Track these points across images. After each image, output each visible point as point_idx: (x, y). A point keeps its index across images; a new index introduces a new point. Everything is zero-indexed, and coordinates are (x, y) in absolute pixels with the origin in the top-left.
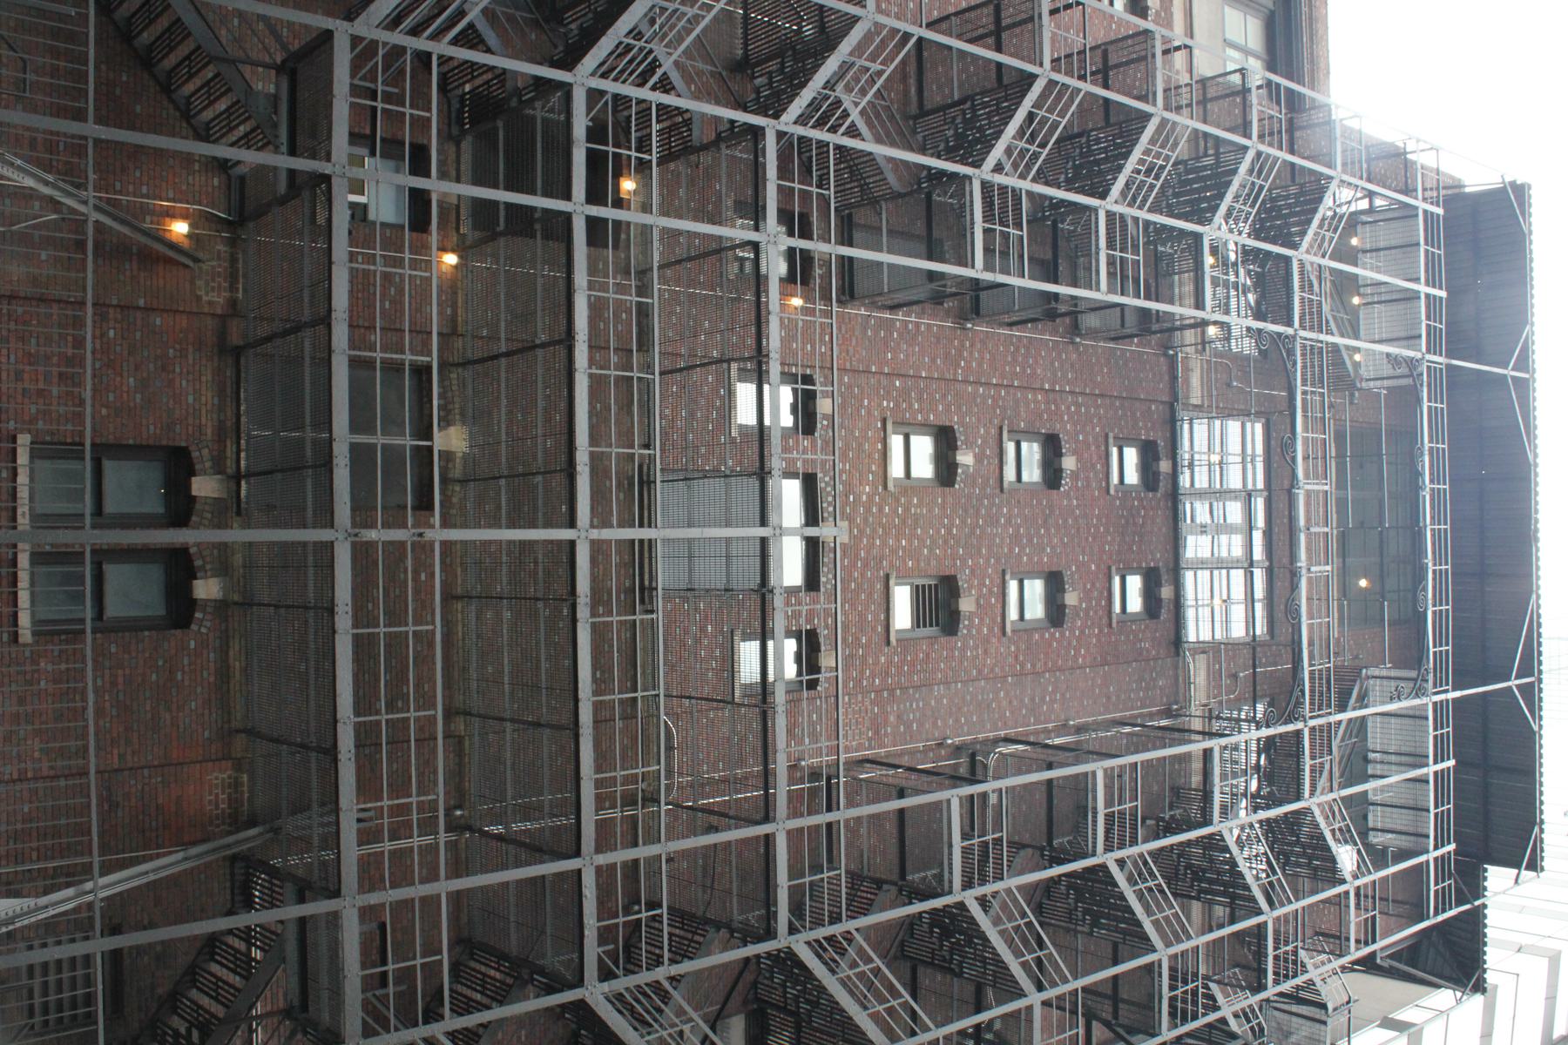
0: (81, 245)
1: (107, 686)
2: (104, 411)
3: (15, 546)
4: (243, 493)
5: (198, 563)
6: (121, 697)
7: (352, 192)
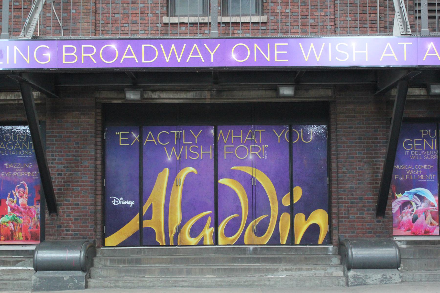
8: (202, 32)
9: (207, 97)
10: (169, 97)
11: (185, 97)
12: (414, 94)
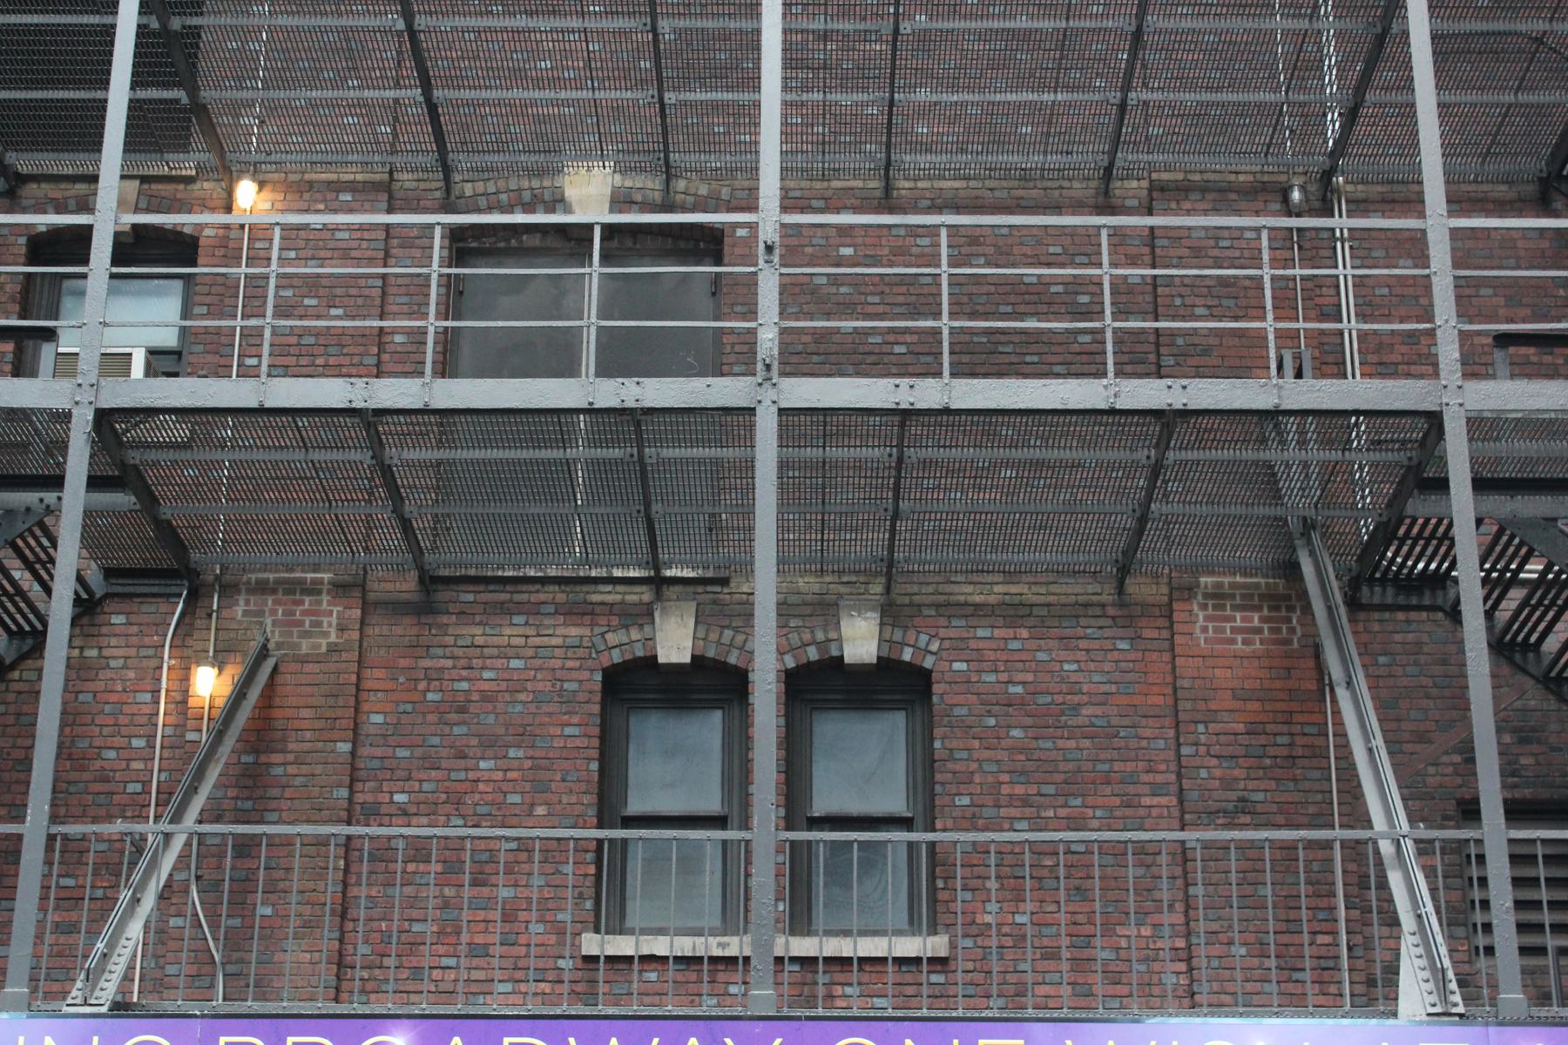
0: (245, 847)
1: (1028, 811)
2: (540, 810)
3: (779, 960)
4: (688, 573)
5: (813, 654)
6: (1051, 789)
7: (127, 373)
8: (720, 988)
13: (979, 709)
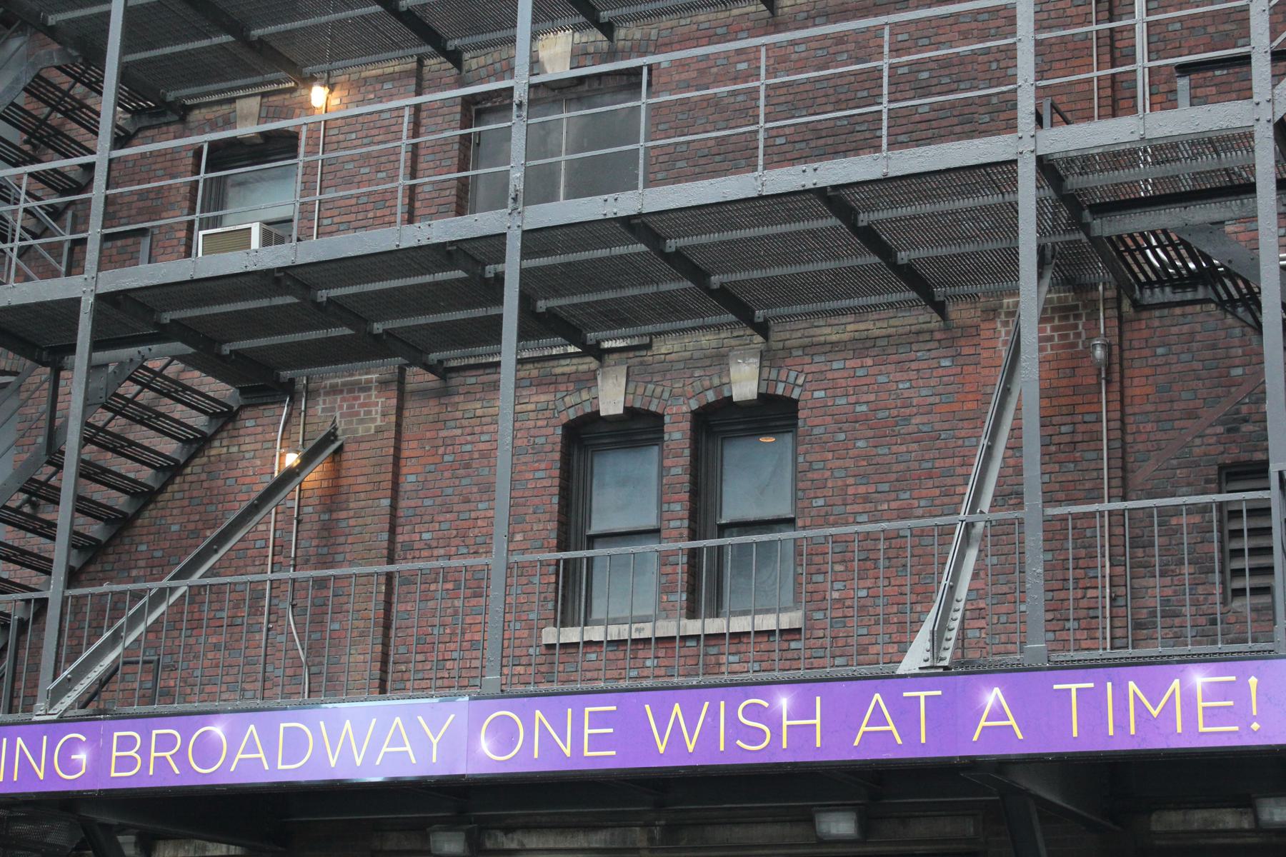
0: (321, 583)
1: (868, 506)
2: (518, 537)
4: (620, 344)
5: (711, 397)
6: (885, 487)
7: (248, 245)
8: (639, 663)
9: (639, 845)
10: (546, 846)
11: (585, 845)
12: (1221, 826)
13: (834, 427)
